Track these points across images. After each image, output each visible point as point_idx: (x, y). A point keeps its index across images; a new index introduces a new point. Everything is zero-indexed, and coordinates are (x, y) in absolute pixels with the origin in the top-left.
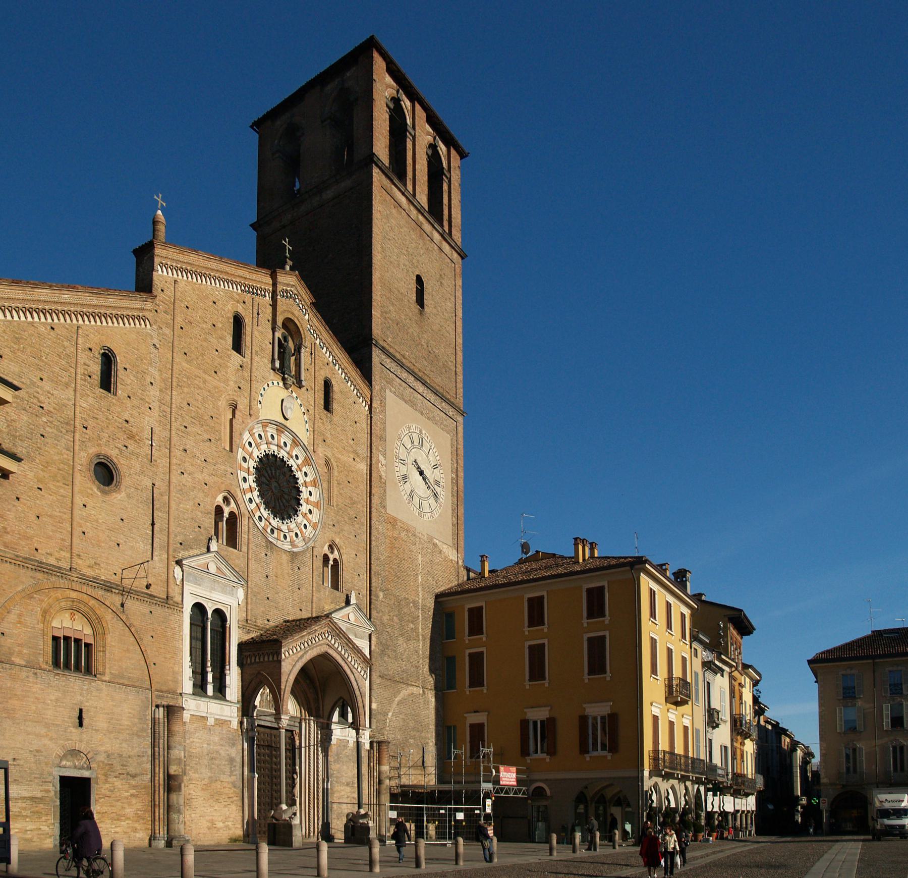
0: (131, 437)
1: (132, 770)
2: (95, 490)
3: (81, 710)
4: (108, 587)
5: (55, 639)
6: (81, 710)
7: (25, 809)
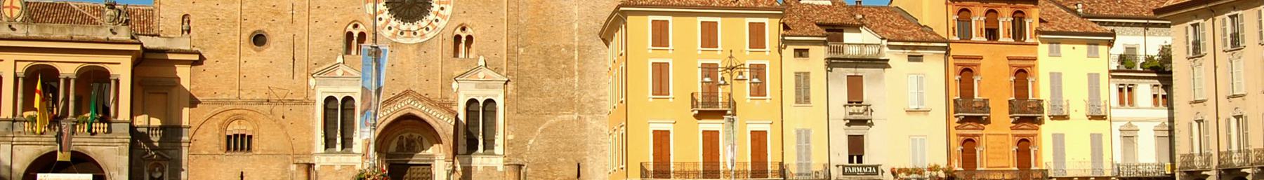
2: (252, 51)
3: (242, 173)
4: (261, 103)
5: (229, 137)
6: (242, 173)
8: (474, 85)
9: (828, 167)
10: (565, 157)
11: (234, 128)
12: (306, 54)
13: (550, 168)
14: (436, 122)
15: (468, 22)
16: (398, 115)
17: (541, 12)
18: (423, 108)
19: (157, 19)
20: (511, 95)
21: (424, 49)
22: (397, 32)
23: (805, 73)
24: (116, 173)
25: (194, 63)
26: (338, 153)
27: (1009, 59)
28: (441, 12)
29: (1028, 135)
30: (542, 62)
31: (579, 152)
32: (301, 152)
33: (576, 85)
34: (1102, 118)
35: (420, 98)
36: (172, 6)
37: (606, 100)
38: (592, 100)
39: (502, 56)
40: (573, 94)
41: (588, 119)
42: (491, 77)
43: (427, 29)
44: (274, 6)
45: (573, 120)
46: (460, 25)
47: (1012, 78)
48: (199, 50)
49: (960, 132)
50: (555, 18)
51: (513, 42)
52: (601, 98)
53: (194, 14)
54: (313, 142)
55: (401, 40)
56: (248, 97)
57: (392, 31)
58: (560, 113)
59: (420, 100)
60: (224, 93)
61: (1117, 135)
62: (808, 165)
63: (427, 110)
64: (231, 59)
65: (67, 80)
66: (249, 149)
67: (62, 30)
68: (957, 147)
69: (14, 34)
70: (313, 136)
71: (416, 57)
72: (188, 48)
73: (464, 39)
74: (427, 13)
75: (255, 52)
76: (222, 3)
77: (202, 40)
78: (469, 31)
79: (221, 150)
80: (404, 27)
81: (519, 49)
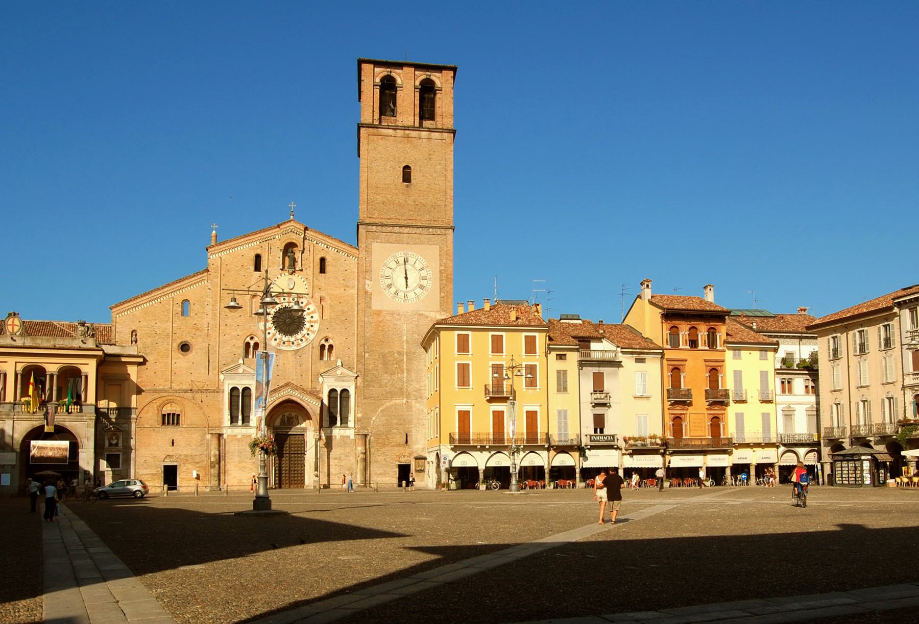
0: (198, 329)
1: (197, 461)
2: (180, 355)
3: (173, 440)
4: (186, 391)
5: (164, 415)
6: (173, 440)
7: (149, 478)
8: (334, 379)
9: (579, 436)
10: (397, 429)
11: (168, 409)
12: (218, 358)
13: (387, 436)
14: (308, 405)
15: (330, 335)
16: (281, 400)
17: (380, 328)
18: (299, 395)
19: (114, 333)
20: (359, 387)
21: (299, 354)
22: (281, 342)
23: (563, 371)
24: (86, 440)
25: (140, 364)
26: (240, 426)
27: (705, 361)
28: (311, 328)
29: (719, 414)
30: (381, 363)
31: (407, 426)
32: (214, 426)
33: (405, 379)
34: (770, 402)
35: (296, 388)
36: (125, 324)
37: (426, 390)
38: (416, 389)
39: (353, 359)
40: (403, 385)
41: (413, 403)
42: (346, 373)
43: (302, 340)
44: (195, 324)
45: (403, 403)
46: (325, 337)
47: (708, 374)
48: (143, 355)
49: (671, 412)
50: (390, 332)
51: (361, 349)
52: (422, 388)
53: (139, 329)
54: (222, 418)
55: (283, 348)
56: (177, 388)
57: (277, 341)
58: (393, 398)
59: (296, 389)
60: (160, 385)
61: (780, 413)
62: (566, 435)
63: (301, 397)
64: (165, 361)
65: (52, 376)
66: (178, 423)
67: (48, 341)
68: (669, 423)
69: (14, 344)
70: (222, 415)
71: (294, 360)
72: (135, 353)
73: (327, 347)
74: (302, 329)
75: (182, 356)
76: (160, 322)
77: (145, 348)
78: (331, 342)
79: (158, 424)
80: (285, 339)
81: (366, 354)
